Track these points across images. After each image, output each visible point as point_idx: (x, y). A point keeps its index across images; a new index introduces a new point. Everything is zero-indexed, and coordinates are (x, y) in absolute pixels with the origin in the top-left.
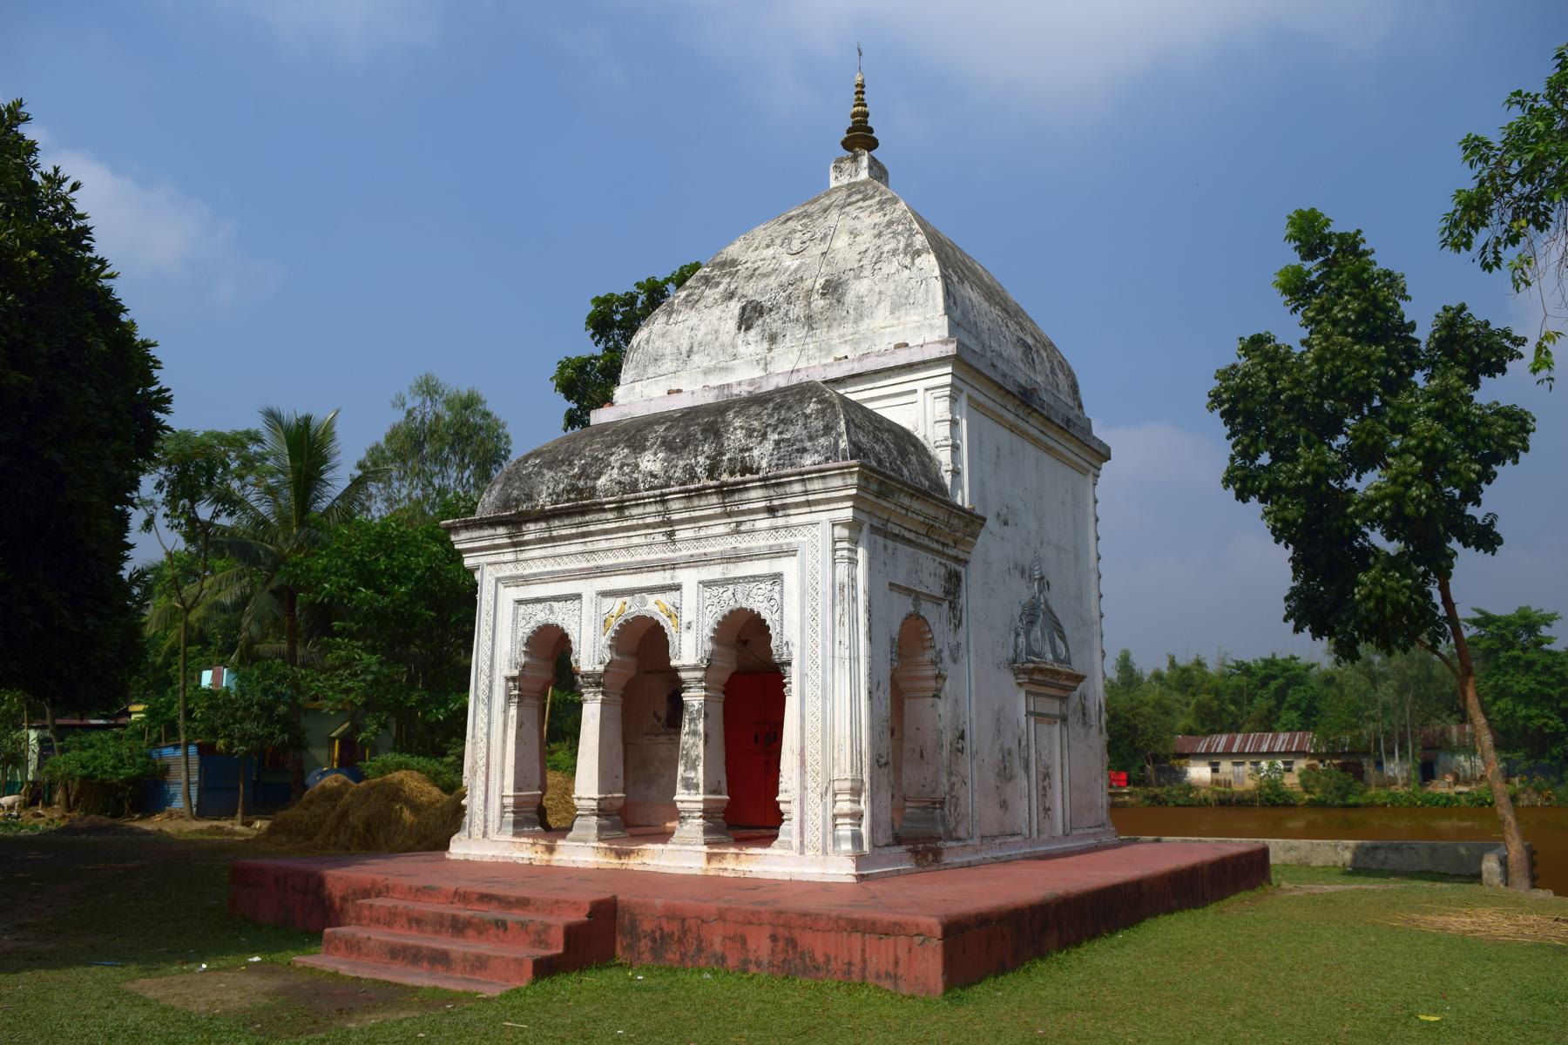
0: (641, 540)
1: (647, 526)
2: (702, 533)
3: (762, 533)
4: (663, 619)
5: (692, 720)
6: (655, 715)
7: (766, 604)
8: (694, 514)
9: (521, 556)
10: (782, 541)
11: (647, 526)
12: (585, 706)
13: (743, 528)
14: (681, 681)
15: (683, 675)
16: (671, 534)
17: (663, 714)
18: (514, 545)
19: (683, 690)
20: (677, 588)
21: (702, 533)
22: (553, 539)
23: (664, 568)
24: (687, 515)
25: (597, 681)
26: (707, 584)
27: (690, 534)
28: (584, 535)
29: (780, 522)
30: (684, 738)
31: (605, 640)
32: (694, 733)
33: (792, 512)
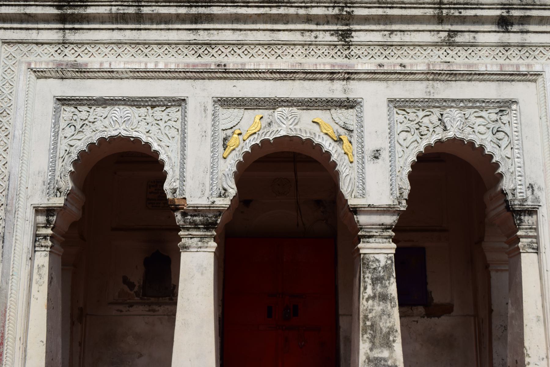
0: (296, 37)
1: (309, 19)
2: (396, 38)
3: (485, 50)
4: (327, 145)
5: (375, 281)
6: (125, 281)
7: (489, 136)
8: (390, 12)
9: (71, 37)
10: (514, 61)
11: (309, 19)
12: (185, 257)
13: (459, 39)
14: (356, 227)
15: (362, 219)
16: (345, 35)
17: (137, 276)
18: (62, 19)
19: (359, 239)
20: (349, 104)
21: (396, 38)
22: (139, 18)
23: (331, 75)
24: (380, 12)
25: (206, 220)
26: (399, 104)
27: (377, 37)
28: (196, 19)
29: (514, 38)
30: (364, 304)
31: (229, 166)
32: (384, 298)
33: (532, 28)
